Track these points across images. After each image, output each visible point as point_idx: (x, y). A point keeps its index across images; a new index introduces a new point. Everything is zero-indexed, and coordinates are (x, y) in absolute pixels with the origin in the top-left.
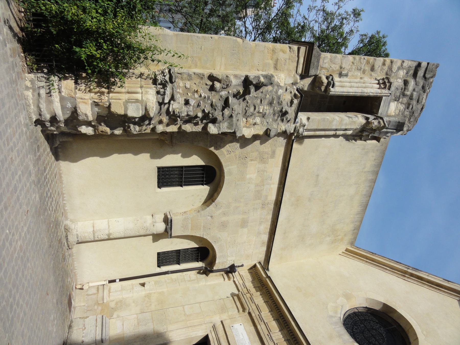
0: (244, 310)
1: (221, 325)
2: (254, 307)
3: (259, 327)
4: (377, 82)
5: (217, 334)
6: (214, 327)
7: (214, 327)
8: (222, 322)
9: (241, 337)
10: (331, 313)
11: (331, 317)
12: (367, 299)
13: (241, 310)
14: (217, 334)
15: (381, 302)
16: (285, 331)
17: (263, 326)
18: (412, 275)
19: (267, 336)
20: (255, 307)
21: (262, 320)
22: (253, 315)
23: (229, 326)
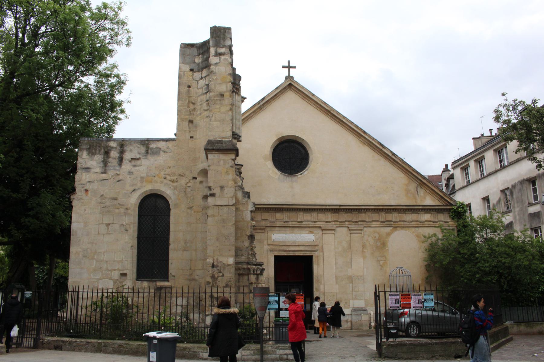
0: (264, 229)
1: (271, 246)
2: (264, 222)
3: (278, 225)
4: (235, 94)
5: (276, 251)
6: (271, 251)
7: (271, 251)
8: (268, 245)
9: (281, 237)
10: (277, 177)
11: (279, 178)
12: (271, 147)
13: (263, 231)
14: (276, 251)
15: (276, 140)
16: (285, 212)
17: (278, 223)
18: (263, 104)
19: (285, 223)
20: (263, 222)
21: (274, 222)
22: (269, 225)
23: (273, 242)
